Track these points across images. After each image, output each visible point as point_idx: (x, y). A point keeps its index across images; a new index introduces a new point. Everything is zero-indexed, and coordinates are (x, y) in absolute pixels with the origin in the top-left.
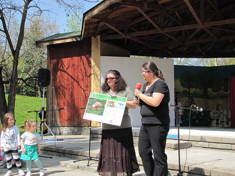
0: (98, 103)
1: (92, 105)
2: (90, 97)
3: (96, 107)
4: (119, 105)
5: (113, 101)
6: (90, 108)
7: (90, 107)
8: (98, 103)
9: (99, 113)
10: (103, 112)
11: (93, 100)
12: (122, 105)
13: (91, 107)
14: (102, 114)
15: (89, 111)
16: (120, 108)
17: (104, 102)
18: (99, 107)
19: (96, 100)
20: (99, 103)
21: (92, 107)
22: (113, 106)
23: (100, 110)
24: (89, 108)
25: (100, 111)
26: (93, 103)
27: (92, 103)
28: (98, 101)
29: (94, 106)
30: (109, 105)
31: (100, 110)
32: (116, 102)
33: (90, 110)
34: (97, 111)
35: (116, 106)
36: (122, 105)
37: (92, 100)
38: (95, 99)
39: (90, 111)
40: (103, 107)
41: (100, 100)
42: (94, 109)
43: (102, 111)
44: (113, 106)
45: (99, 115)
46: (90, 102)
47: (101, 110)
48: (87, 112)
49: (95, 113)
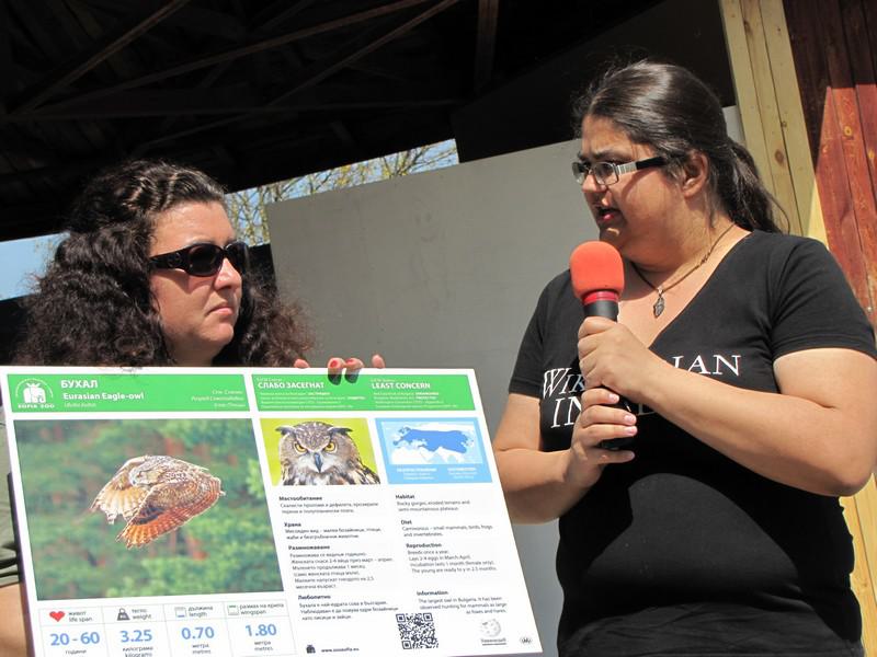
0: (155, 463)
1: (84, 498)
2: (10, 418)
3: (150, 513)
4: (413, 455)
5: (337, 418)
6: (80, 532)
7: (76, 526)
8: (147, 474)
9: (222, 565)
10: (265, 549)
11: (77, 444)
12: (455, 441)
13: (82, 520)
14: (264, 576)
15: (84, 571)
16: (442, 475)
17: (230, 444)
18: (199, 505)
19: (118, 441)
20: (170, 463)
21: (103, 523)
22: (353, 469)
23: (228, 538)
24: (76, 543)
25: (232, 548)
26: (93, 471)
27: (78, 477)
28: (151, 440)
29: (114, 503)
30: (307, 463)
31: (228, 538)
32: (371, 426)
33: (93, 562)
34: (183, 553)
35: (391, 469)
36: (455, 441)
37: (61, 451)
38: (104, 433)
39: (96, 573)
40: (247, 498)
41: (162, 430)
42: (134, 537)
43: (249, 547)
44: (354, 475)
45: (228, 588)
46: (43, 476)
47: (241, 537)
48: (61, 594)
49: (168, 579)
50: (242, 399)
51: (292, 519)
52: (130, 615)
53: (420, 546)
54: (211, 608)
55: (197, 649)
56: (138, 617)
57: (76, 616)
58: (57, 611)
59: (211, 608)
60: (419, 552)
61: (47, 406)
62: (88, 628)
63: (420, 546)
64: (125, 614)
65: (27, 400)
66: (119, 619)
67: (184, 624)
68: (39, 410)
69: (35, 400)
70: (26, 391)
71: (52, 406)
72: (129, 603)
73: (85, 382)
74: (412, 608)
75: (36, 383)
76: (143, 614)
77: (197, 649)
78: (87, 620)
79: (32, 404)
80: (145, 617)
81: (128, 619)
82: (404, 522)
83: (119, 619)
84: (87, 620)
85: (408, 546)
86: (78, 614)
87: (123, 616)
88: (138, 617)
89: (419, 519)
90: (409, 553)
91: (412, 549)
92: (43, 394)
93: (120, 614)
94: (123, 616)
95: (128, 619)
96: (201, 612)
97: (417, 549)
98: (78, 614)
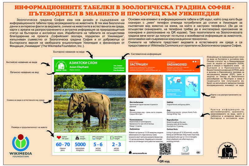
50: (124, 68)
51: (132, 109)
52: (79, 138)
53: (171, 120)
54: (103, 137)
55: (97, 149)
56: (81, 139)
57: (64, 138)
58: (59, 136)
59: (103, 137)
60: (170, 122)
61: (64, 70)
62: (67, 141)
63: (171, 120)
64: (78, 137)
65: (59, 68)
66: (76, 139)
67: (95, 141)
68: (62, 71)
69: (61, 68)
70: (59, 65)
71: (66, 70)
72: (80, 134)
73: (77, 62)
74: (165, 141)
75: (62, 62)
76: (83, 138)
77: (97, 149)
78: (67, 139)
79: (60, 69)
80: (83, 139)
81: (79, 139)
82: (168, 110)
83: (76, 139)
84: (67, 139)
85: (167, 120)
86: (65, 137)
87: (77, 138)
88: (81, 139)
89: (173, 109)
90: (167, 122)
91: (168, 121)
92: (64, 66)
93: (77, 137)
94: (77, 138)
95: (79, 139)
96: (100, 138)
97: (170, 121)
98: (65, 137)
